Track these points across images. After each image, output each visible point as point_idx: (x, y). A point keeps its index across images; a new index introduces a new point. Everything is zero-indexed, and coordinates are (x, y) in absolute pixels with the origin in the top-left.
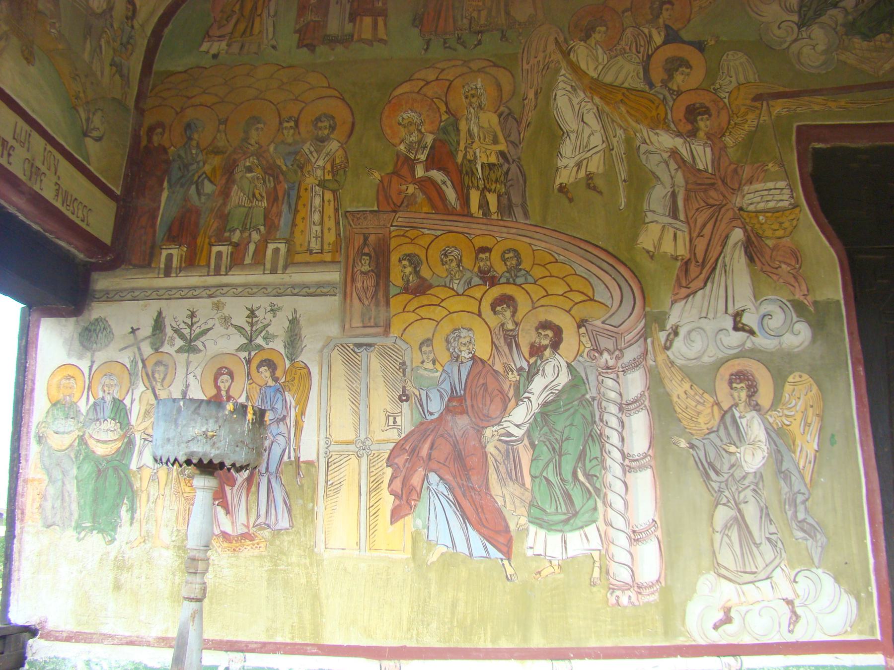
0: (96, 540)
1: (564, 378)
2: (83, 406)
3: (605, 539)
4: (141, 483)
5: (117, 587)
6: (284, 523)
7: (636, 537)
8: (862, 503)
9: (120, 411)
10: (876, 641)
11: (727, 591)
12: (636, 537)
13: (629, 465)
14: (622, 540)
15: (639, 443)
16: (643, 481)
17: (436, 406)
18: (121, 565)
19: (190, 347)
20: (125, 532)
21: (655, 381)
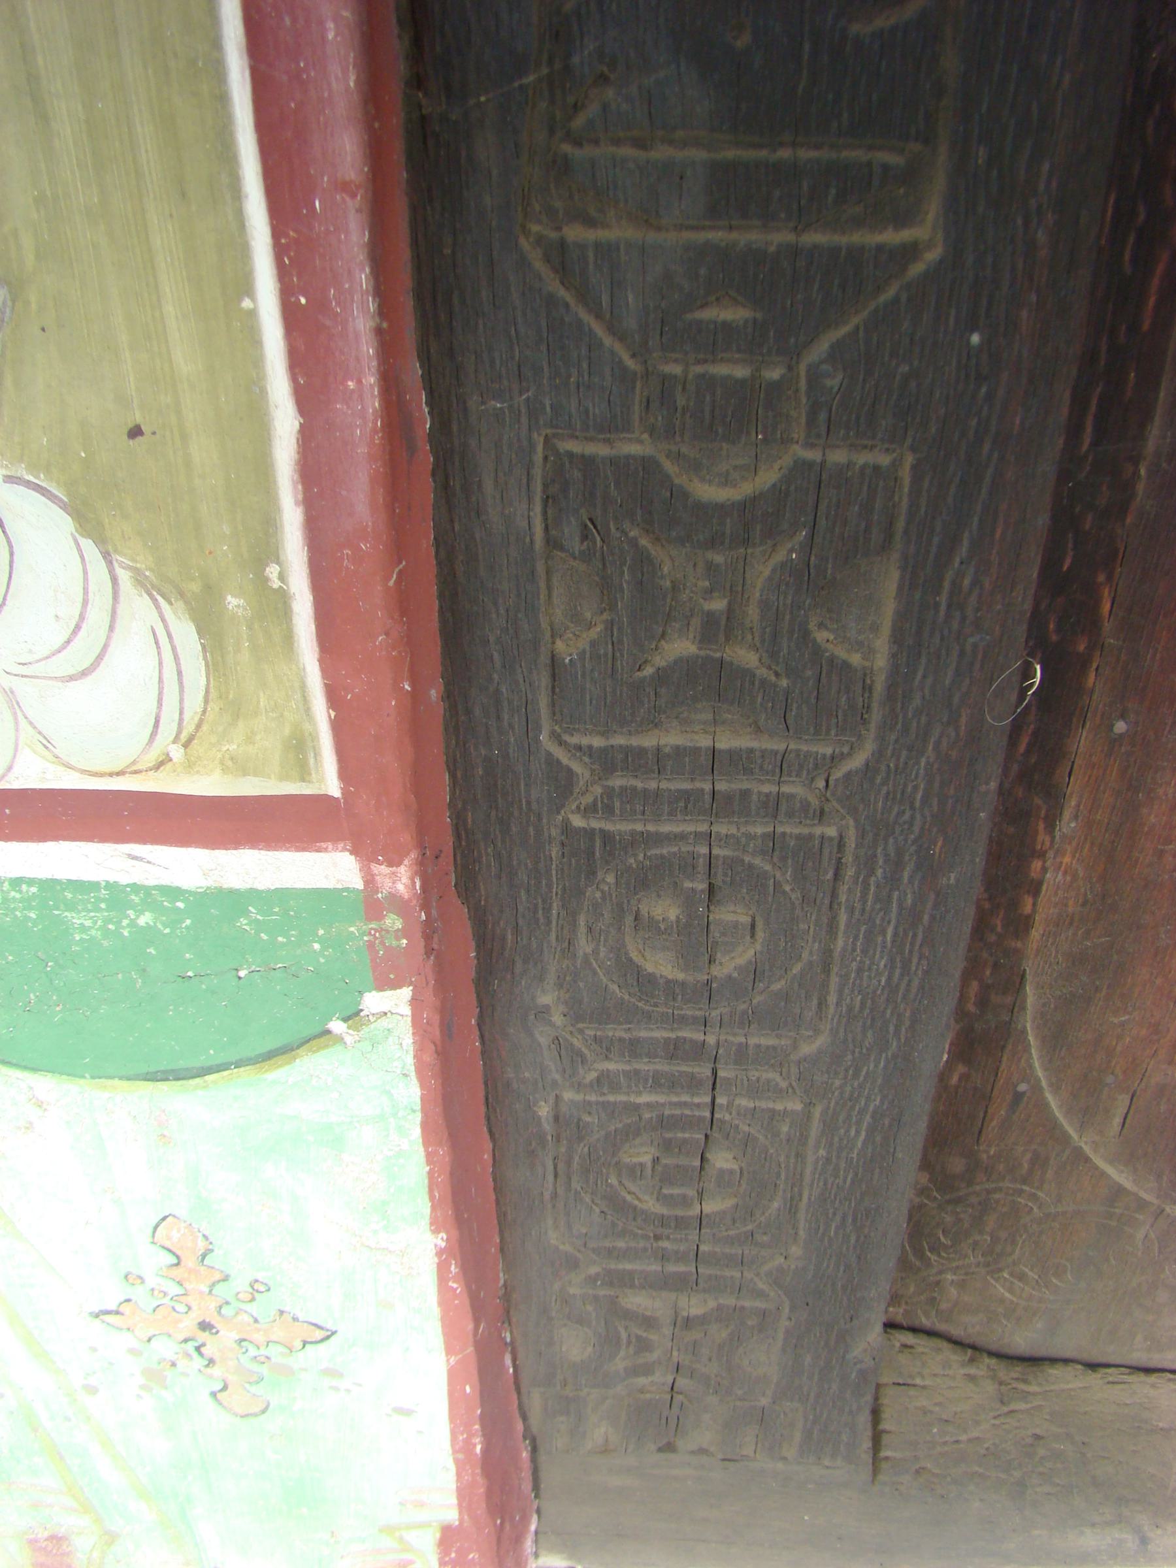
8: (217, 44)
10: (324, 800)
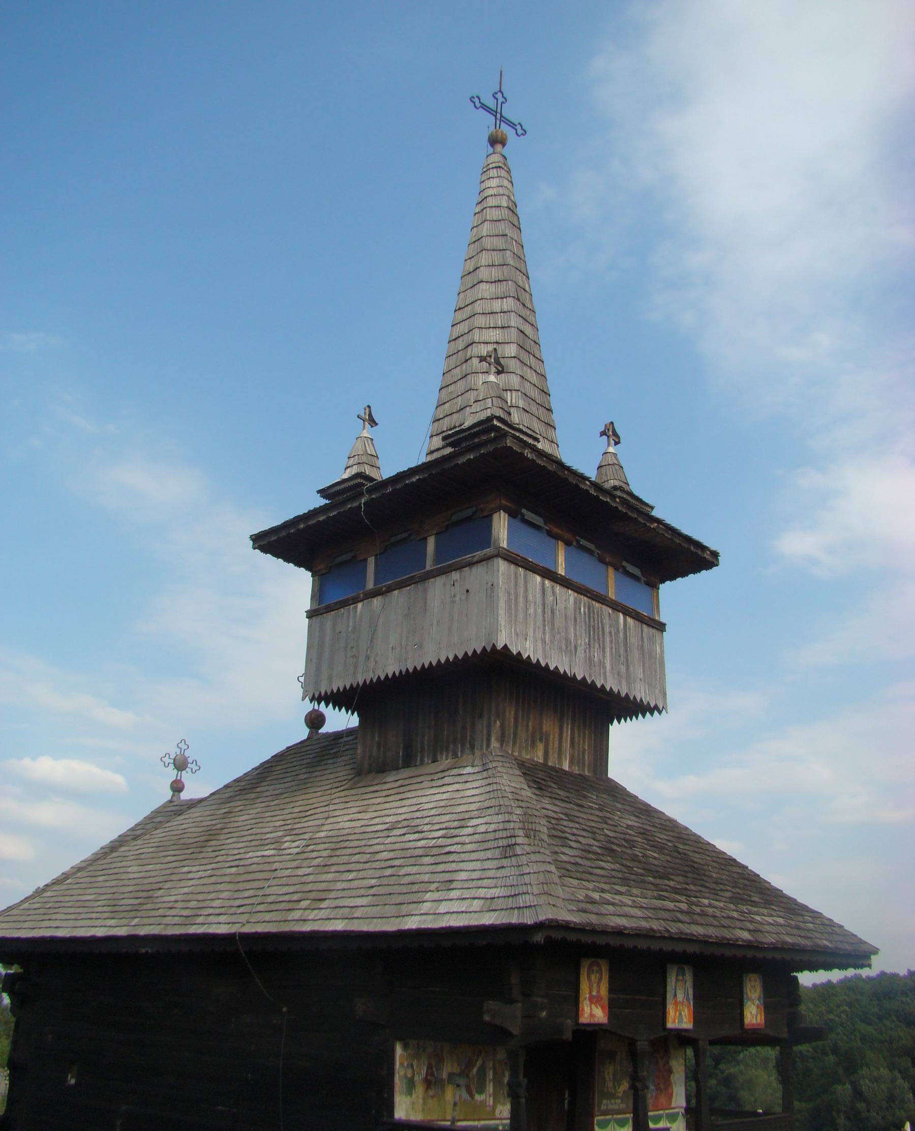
0: (409, 1097)
1: (481, 1062)
2: (406, 1064)
3: (486, 1097)
4: (416, 1084)
5: (413, 1108)
6: (440, 1093)
7: (490, 1096)
9: (412, 1066)
11: (501, 1107)
12: (490, 1096)
14: (488, 1096)
15: (491, 1077)
17: (463, 1067)
18: (413, 1103)
19: (424, 1051)
20: (414, 1095)
21: (494, 1064)
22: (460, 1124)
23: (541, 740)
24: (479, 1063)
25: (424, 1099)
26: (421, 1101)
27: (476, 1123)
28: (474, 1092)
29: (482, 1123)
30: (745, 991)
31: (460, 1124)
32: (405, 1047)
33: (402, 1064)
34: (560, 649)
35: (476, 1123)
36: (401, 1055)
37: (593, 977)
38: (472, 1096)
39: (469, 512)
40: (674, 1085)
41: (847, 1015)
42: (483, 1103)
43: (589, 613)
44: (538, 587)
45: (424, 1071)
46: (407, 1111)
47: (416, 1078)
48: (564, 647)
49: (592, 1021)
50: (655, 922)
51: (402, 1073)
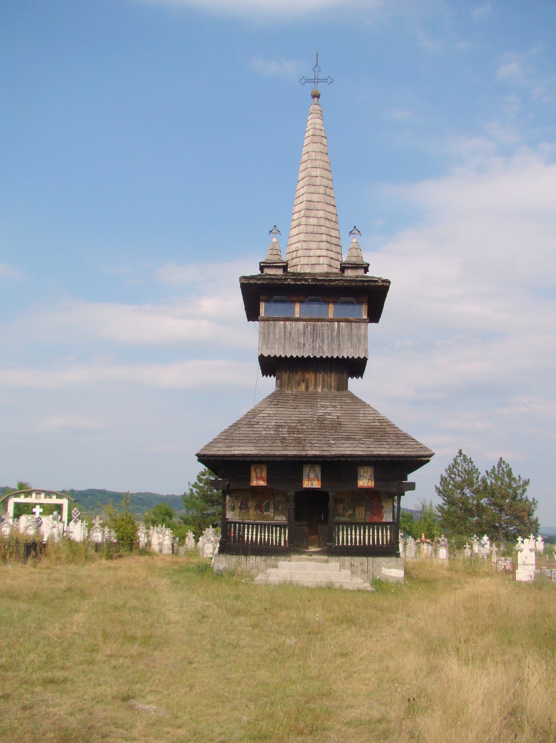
0: (232, 513)
9: (234, 503)
13: (272, 508)
15: (272, 506)
16: (272, 509)
22: (245, 521)
23: (303, 382)
24: (266, 502)
25: (239, 513)
26: (238, 514)
27: (265, 521)
28: (263, 511)
29: (268, 521)
30: (359, 472)
31: (245, 521)
32: (231, 496)
33: (229, 502)
34: (295, 347)
35: (265, 521)
36: (229, 499)
37: (258, 471)
38: (263, 513)
39: (349, 273)
40: (384, 514)
41: (502, 484)
42: (268, 515)
43: (314, 330)
44: (282, 327)
45: (239, 504)
46: (232, 516)
47: (236, 506)
48: (296, 346)
49: (258, 485)
50: (256, 451)
51: (229, 504)
